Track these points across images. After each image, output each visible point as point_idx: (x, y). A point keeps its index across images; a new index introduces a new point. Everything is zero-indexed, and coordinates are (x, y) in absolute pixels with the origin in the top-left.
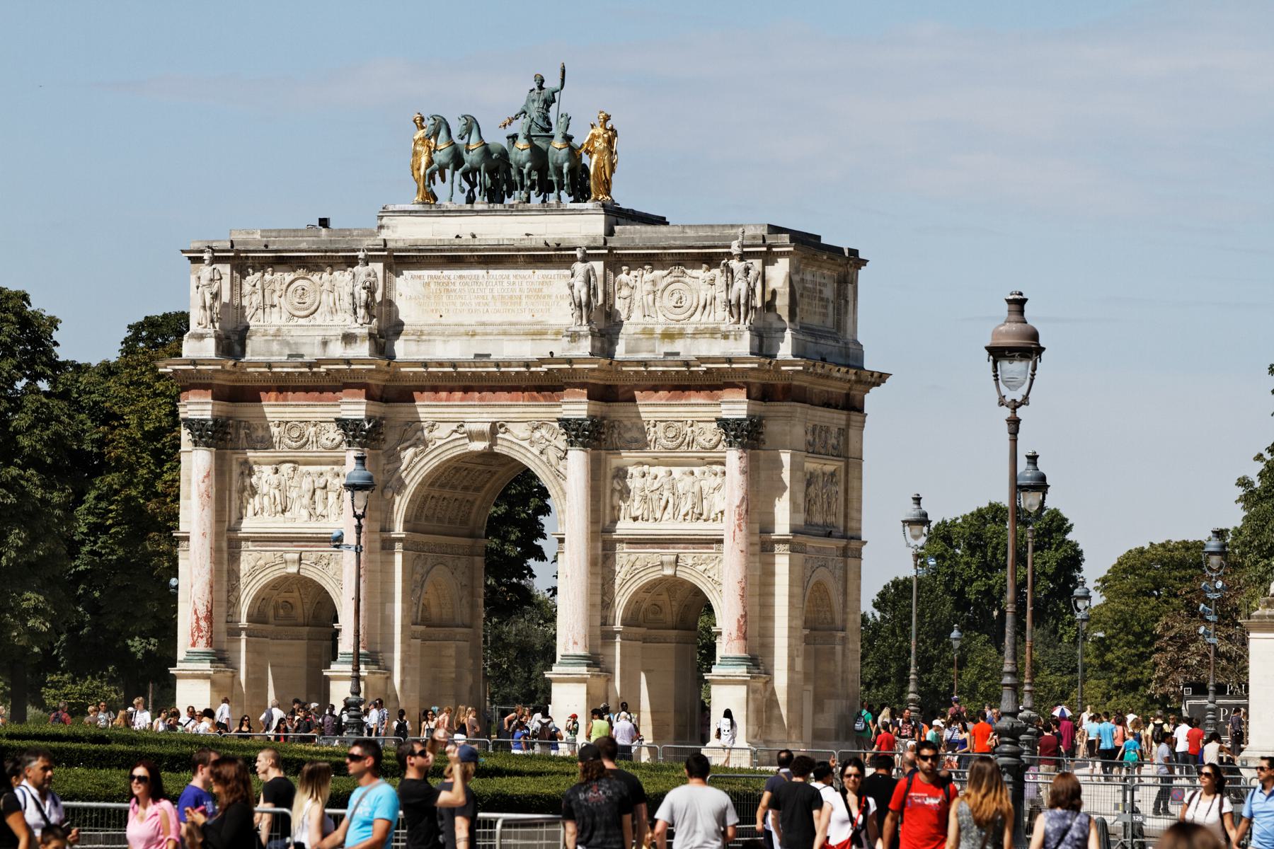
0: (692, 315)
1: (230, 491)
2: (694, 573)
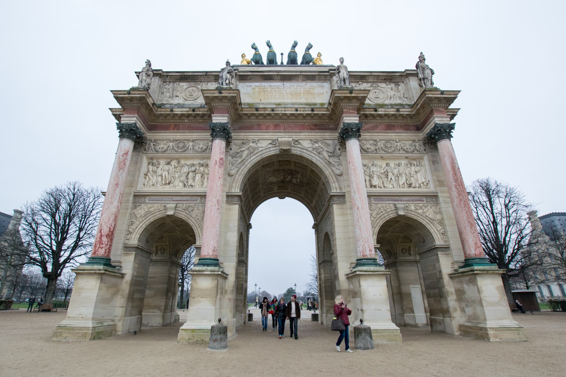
0: (385, 101)
1: (139, 172)
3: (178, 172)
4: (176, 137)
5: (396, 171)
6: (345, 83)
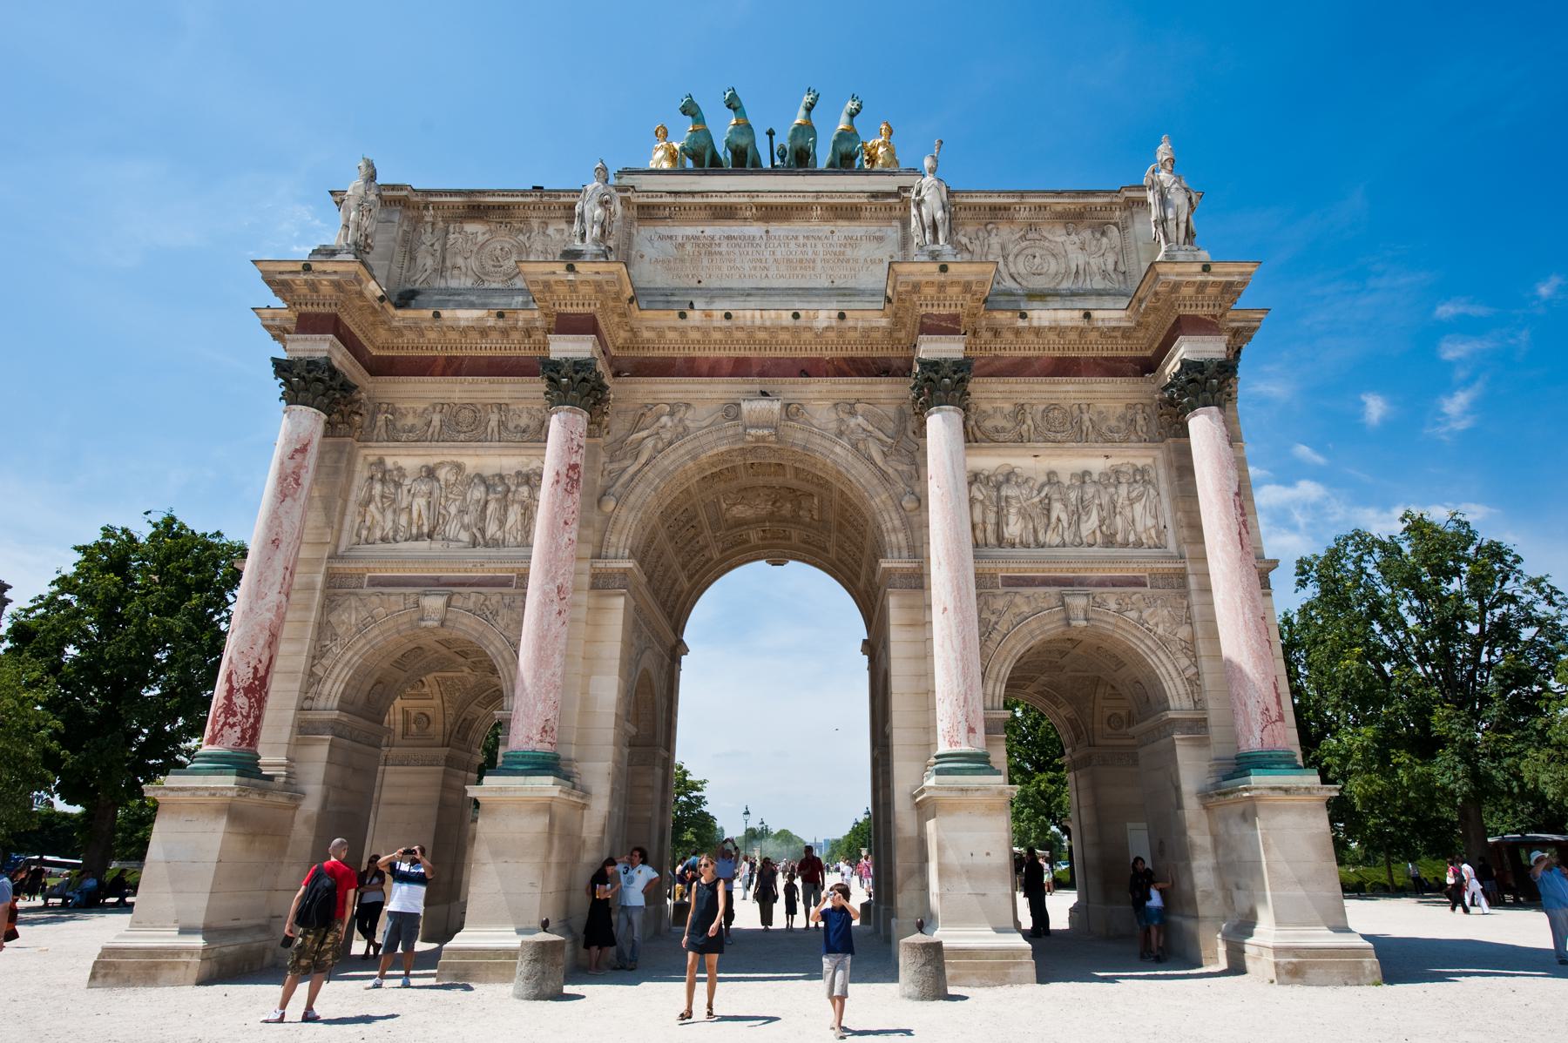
0: (1058, 284)
2: (1121, 624)
3: (455, 500)
4: (452, 395)
5: (1073, 496)
6: (935, 240)
